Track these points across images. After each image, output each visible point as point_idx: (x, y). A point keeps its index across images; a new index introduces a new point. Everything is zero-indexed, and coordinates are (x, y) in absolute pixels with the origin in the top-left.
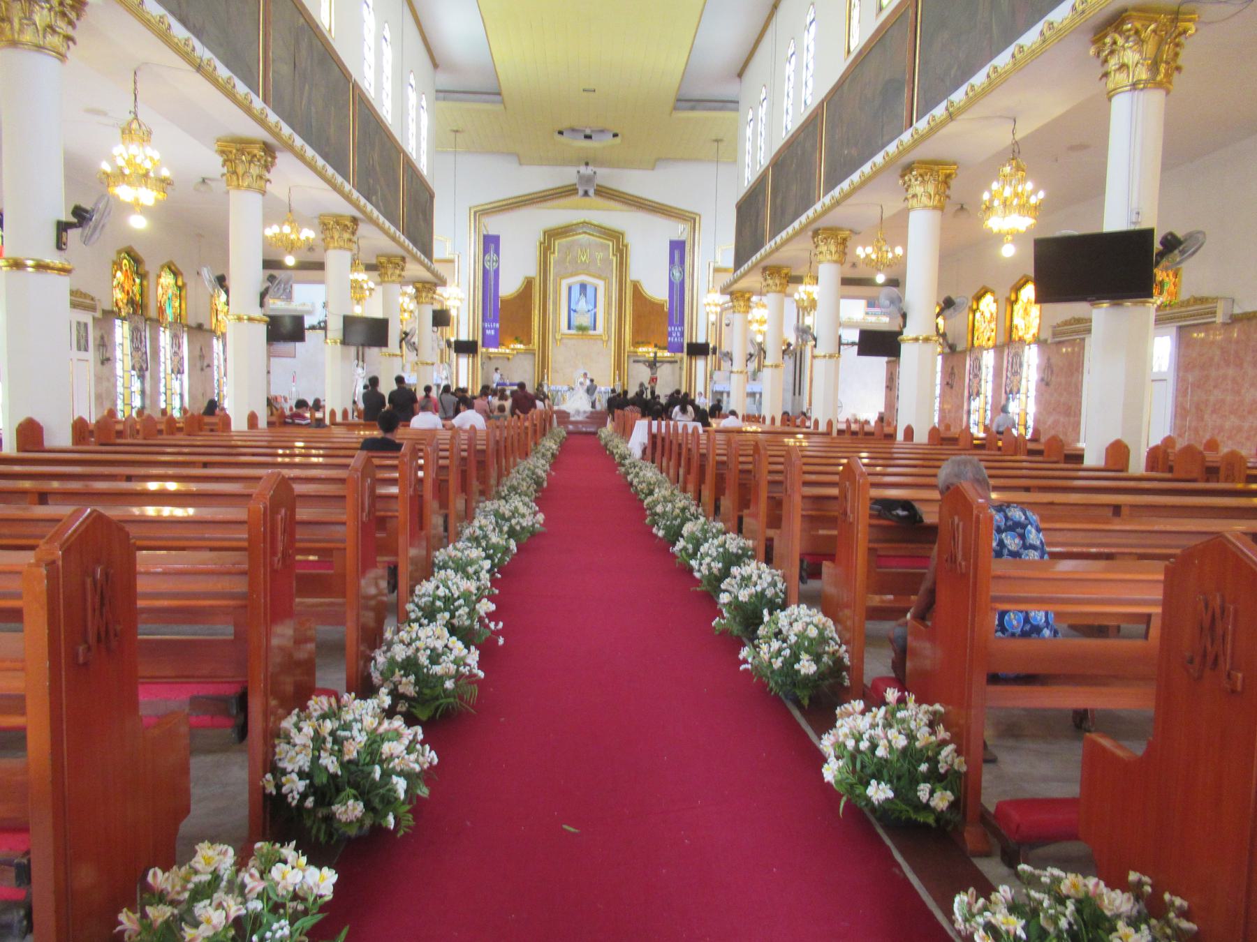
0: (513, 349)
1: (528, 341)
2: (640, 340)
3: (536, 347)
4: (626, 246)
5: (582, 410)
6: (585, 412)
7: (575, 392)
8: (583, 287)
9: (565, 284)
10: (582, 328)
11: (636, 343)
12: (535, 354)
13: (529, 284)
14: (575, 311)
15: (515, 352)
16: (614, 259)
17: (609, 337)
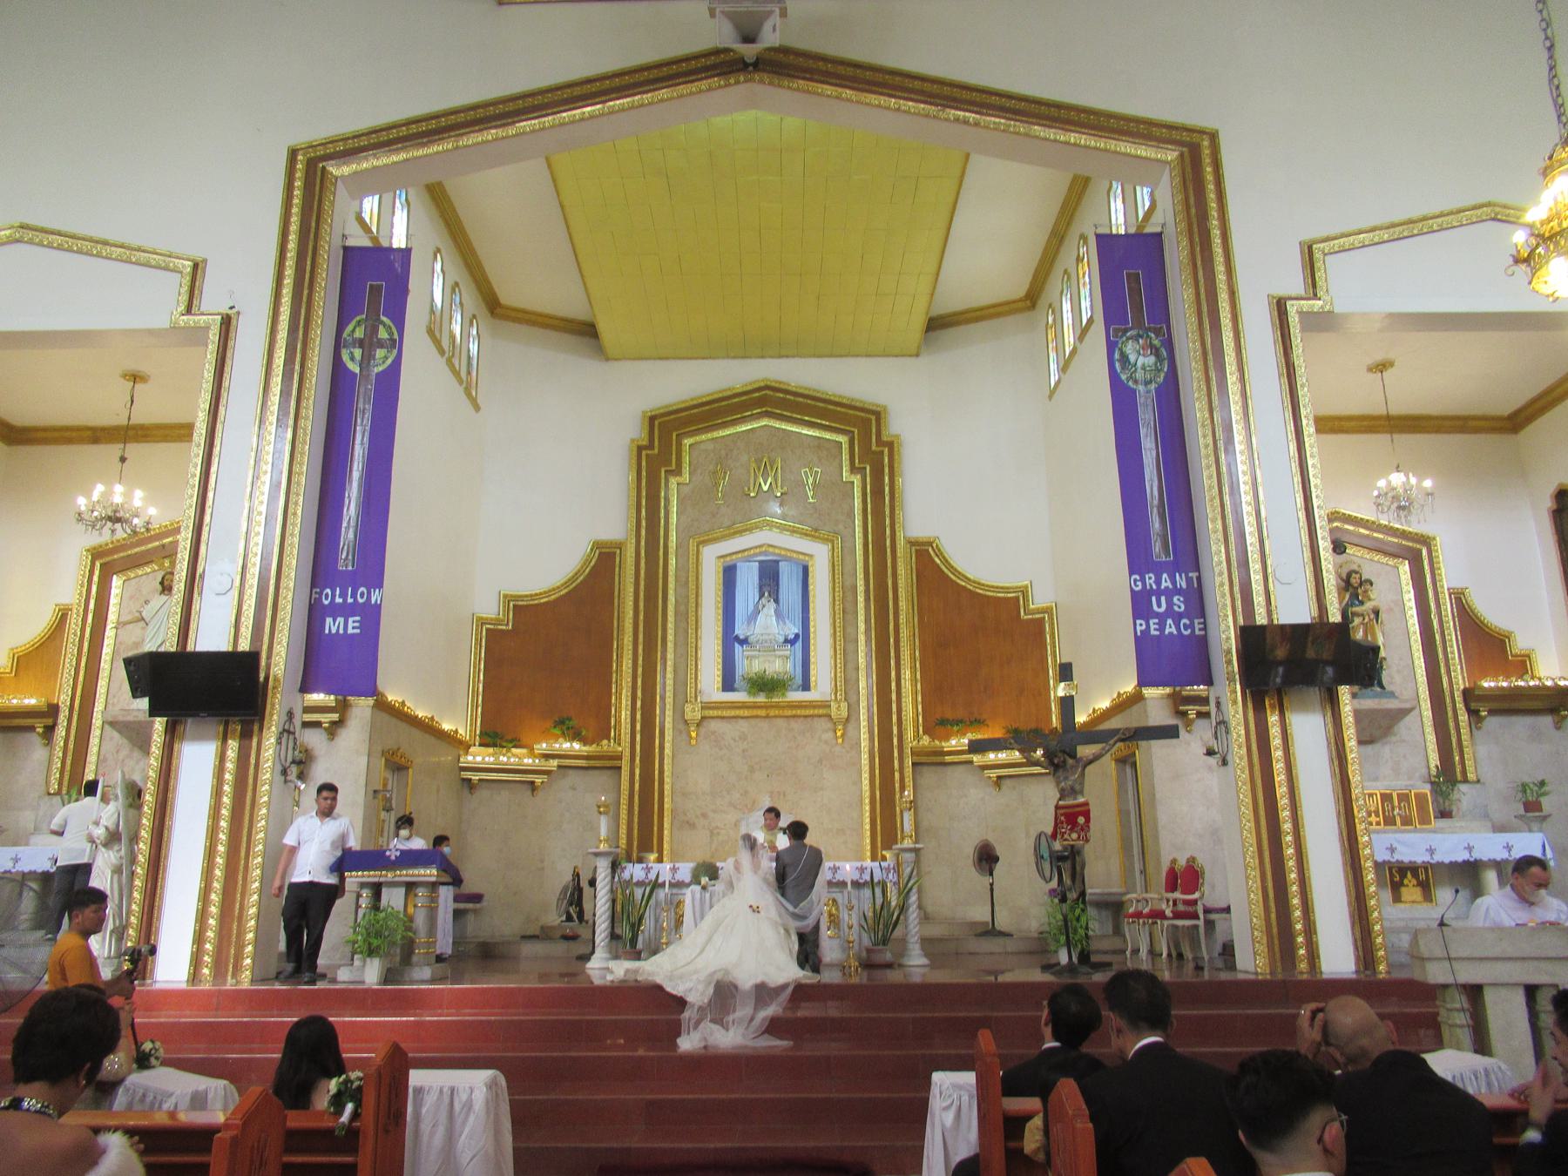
0: (547, 757)
1: (604, 732)
2: (949, 715)
3: (624, 748)
4: (890, 445)
5: (746, 979)
6: (763, 993)
7: (719, 886)
8: (769, 578)
9: (711, 559)
10: (765, 685)
11: (937, 724)
12: (620, 768)
13: (605, 559)
14: (744, 642)
15: (554, 763)
16: (857, 479)
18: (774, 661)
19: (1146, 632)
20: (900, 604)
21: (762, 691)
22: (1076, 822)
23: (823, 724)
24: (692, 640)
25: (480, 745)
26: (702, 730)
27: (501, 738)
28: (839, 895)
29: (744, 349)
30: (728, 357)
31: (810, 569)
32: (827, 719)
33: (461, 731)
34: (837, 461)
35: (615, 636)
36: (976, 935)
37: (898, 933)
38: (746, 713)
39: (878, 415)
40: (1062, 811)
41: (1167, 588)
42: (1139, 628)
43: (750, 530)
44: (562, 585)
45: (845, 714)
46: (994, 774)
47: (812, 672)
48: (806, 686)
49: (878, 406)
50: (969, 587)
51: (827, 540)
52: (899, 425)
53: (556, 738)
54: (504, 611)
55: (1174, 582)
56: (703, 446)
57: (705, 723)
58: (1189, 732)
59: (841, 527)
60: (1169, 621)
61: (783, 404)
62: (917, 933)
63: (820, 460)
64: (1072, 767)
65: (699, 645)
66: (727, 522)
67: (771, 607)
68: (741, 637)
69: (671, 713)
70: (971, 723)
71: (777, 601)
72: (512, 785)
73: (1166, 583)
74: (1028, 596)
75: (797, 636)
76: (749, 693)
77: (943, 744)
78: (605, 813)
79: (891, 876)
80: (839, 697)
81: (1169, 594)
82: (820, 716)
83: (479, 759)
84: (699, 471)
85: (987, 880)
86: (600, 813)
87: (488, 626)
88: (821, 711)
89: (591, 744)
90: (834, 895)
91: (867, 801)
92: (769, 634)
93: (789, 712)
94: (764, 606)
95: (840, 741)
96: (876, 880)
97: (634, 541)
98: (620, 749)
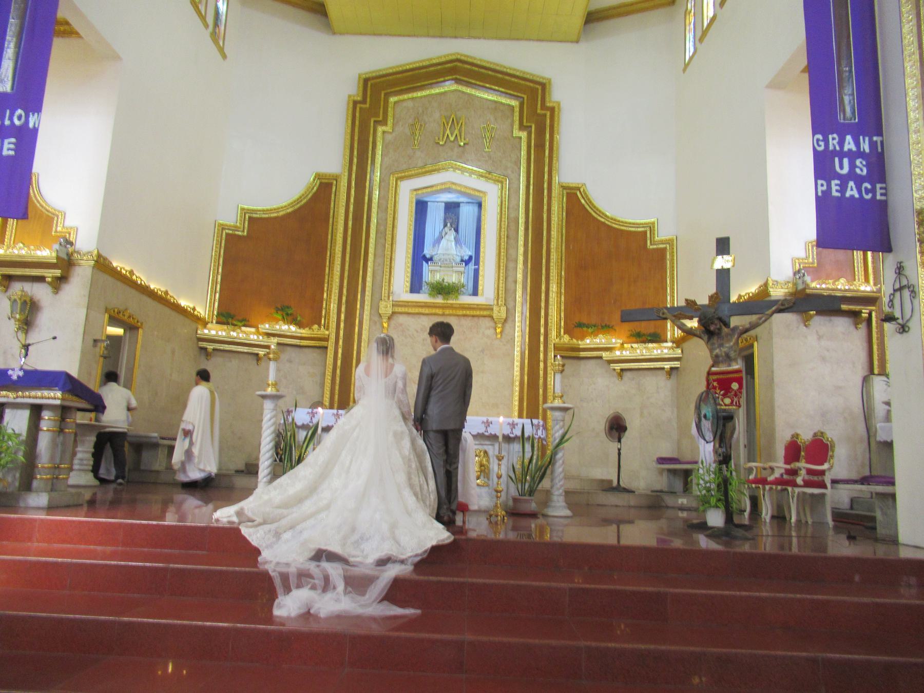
0: (269, 335)
2: (585, 321)
4: (552, 110)
11: (575, 327)
12: (326, 348)
14: (429, 260)
15: (275, 340)
16: (524, 135)
17: (510, 313)
18: (452, 276)
19: (827, 193)
20: (552, 233)
21: (440, 294)
22: (731, 388)
23: (487, 322)
24: (388, 253)
25: (218, 323)
26: (393, 322)
27: (232, 318)
28: (490, 447)
29: (441, 30)
30: (428, 36)
31: (483, 204)
32: (490, 319)
33: (198, 309)
34: (509, 121)
35: (329, 247)
36: (604, 490)
37: (545, 484)
38: (426, 311)
39: (543, 86)
40: (715, 377)
41: (850, 150)
42: (820, 189)
43: (438, 170)
44: (289, 205)
45: (504, 315)
46: (618, 367)
47: (480, 282)
48: (475, 293)
49: (543, 78)
50: (607, 222)
51: (498, 181)
52: (558, 95)
53: (277, 321)
54: (241, 220)
55: (857, 144)
56: (405, 104)
57: (395, 317)
58: (806, 326)
59: (509, 172)
60: (851, 184)
61: (469, 74)
62: (562, 486)
63: (496, 119)
64: (727, 335)
65: (393, 257)
66: (420, 164)
67: (452, 235)
68: (428, 256)
69: (369, 307)
70: (602, 327)
71: (456, 230)
72: (241, 355)
73: (849, 144)
74: (654, 230)
75: (470, 257)
76: (430, 294)
77: (580, 342)
78: (275, 360)
79: (540, 433)
80: (500, 303)
81: (852, 156)
82: (484, 316)
83: (213, 332)
84: (401, 123)
85: (616, 445)
86: (270, 359)
87: (227, 231)
88: (485, 313)
89: (304, 328)
90: (486, 447)
91: (517, 383)
92: (449, 255)
93: (461, 312)
94: (446, 234)
95: (499, 336)
96: (526, 435)
97: (346, 174)
98: (327, 332)
